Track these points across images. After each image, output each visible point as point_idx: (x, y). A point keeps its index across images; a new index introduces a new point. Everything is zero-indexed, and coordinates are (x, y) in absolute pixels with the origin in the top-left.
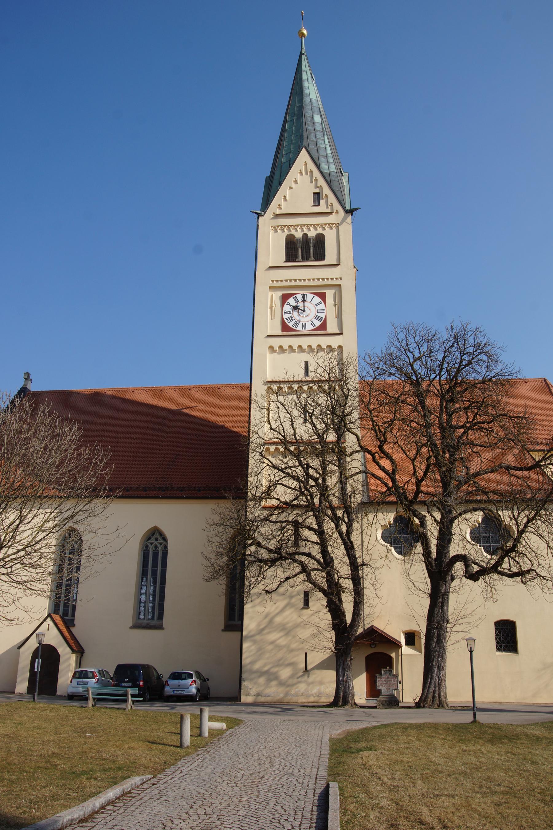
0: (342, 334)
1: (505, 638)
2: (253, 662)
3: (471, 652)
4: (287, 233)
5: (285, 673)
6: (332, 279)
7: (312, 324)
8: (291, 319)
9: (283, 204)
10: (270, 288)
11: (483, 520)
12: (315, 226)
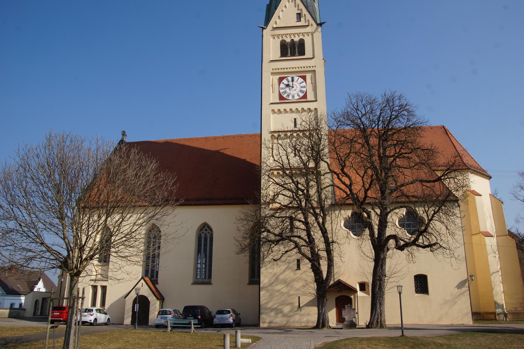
2: (267, 303)
3: (400, 294)
4: (281, 39)
5: (286, 309)
6: (310, 67)
7: (298, 95)
9: (278, 21)
10: (272, 73)
11: (406, 214)
12: (298, 34)
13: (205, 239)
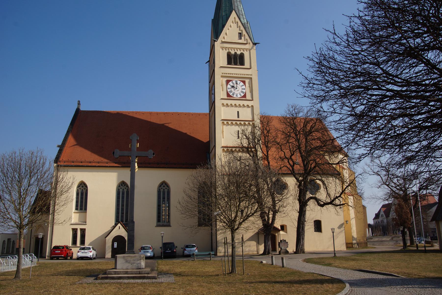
4: (227, 51)
8: (231, 91)
9: (225, 36)
10: (222, 76)
13: (164, 192)
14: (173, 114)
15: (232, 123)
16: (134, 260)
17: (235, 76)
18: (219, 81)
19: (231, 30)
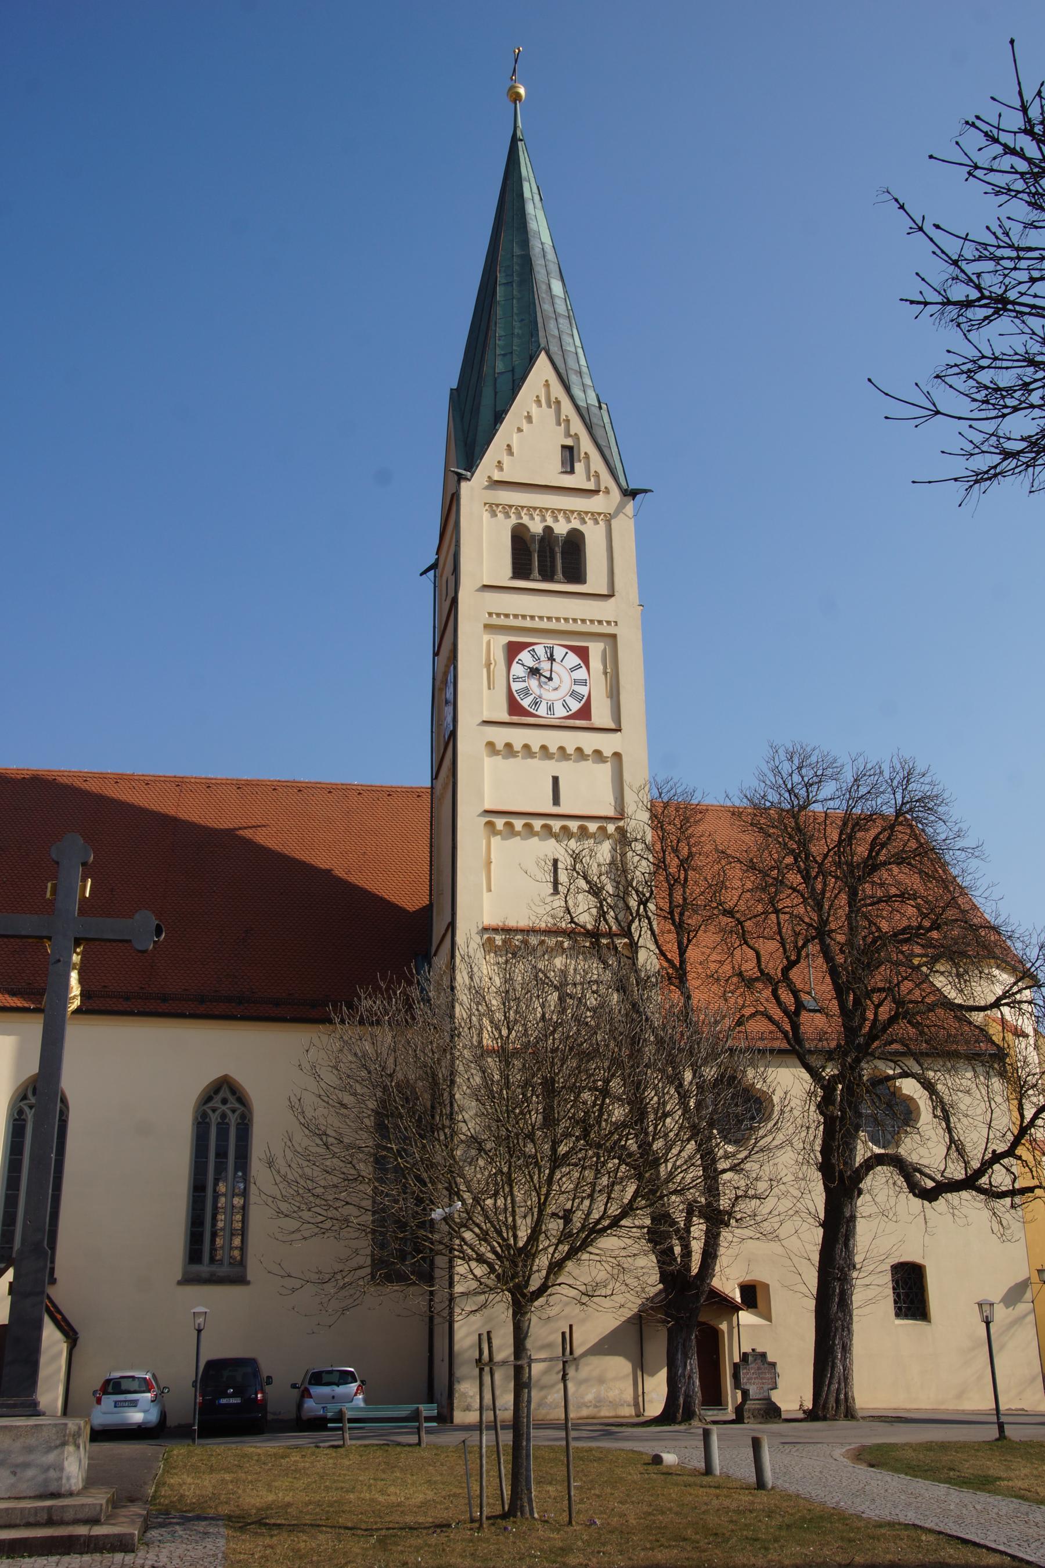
0: (618, 730)
1: (907, 1295)
4: (513, 520)
6: (600, 622)
7: (565, 705)
8: (526, 692)
9: (506, 460)
10: (487, 627)
12: (568, 514)
13: (222, 1126)
14: (275, 787)
15: (528, 826)
16: (30, 1450)
17: (545, 625)
18: (477, 647)
19: (530, 435)
